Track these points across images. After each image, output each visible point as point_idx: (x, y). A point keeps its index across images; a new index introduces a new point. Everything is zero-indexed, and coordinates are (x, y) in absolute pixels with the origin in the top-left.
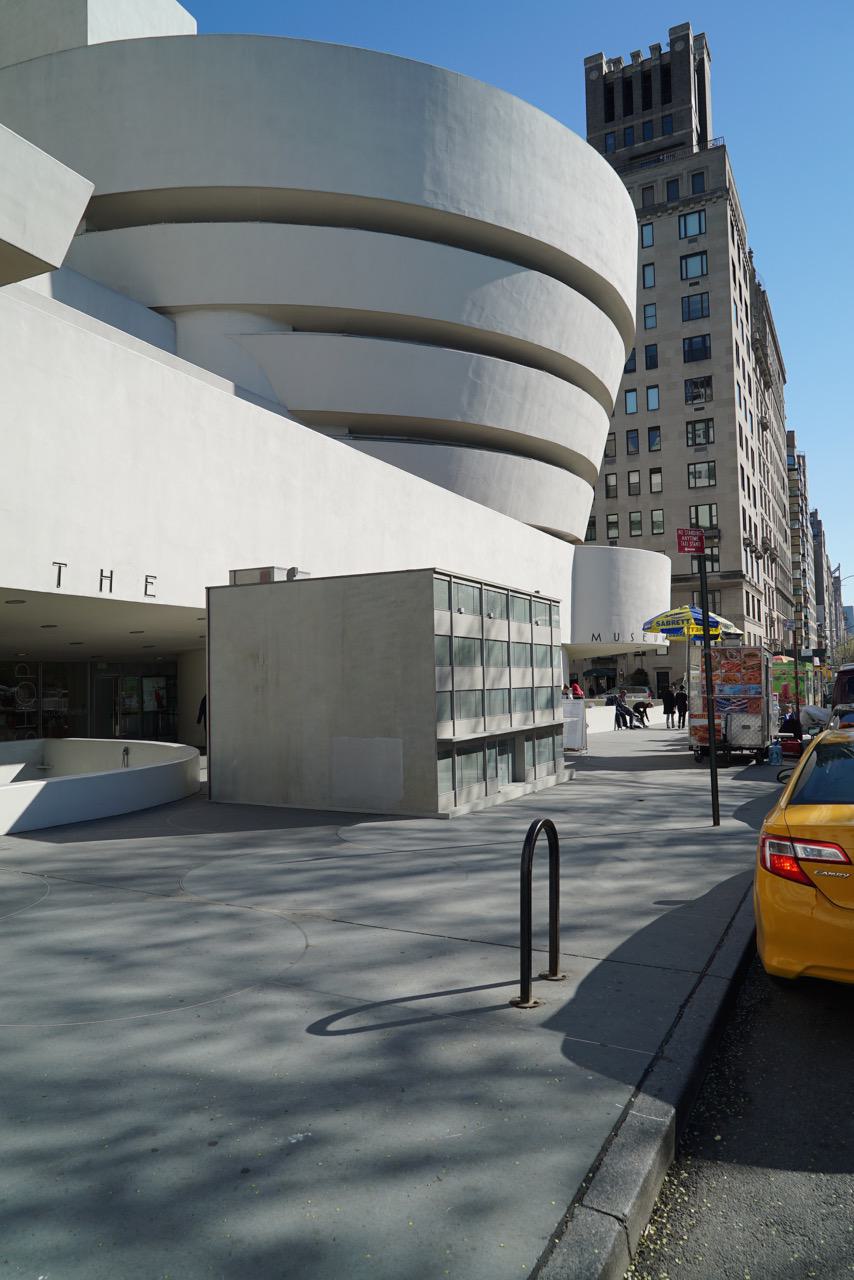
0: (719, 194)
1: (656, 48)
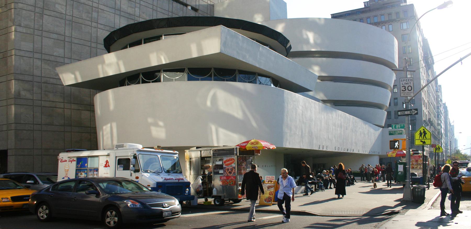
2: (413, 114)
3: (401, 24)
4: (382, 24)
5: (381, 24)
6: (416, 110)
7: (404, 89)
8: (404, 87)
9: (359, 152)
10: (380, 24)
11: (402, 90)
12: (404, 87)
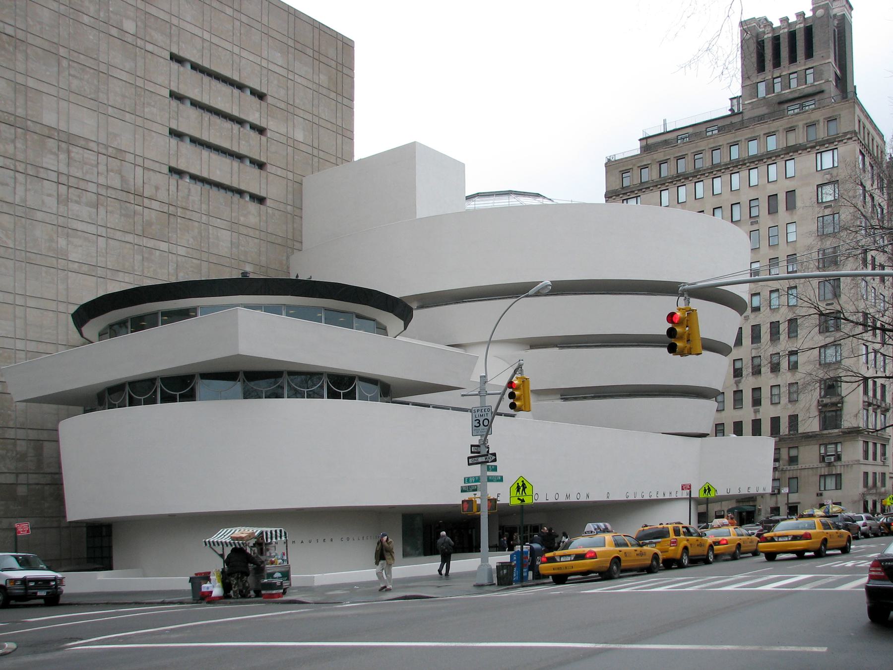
0: (849, 136)
1: (801, 15)
3: (819, 155)
4: (768, 158)
5: (765, 161)
7: (478, 425)
8: (478, 421)
10: (762, 160)
11: (475, 426)
12: (478, 421)
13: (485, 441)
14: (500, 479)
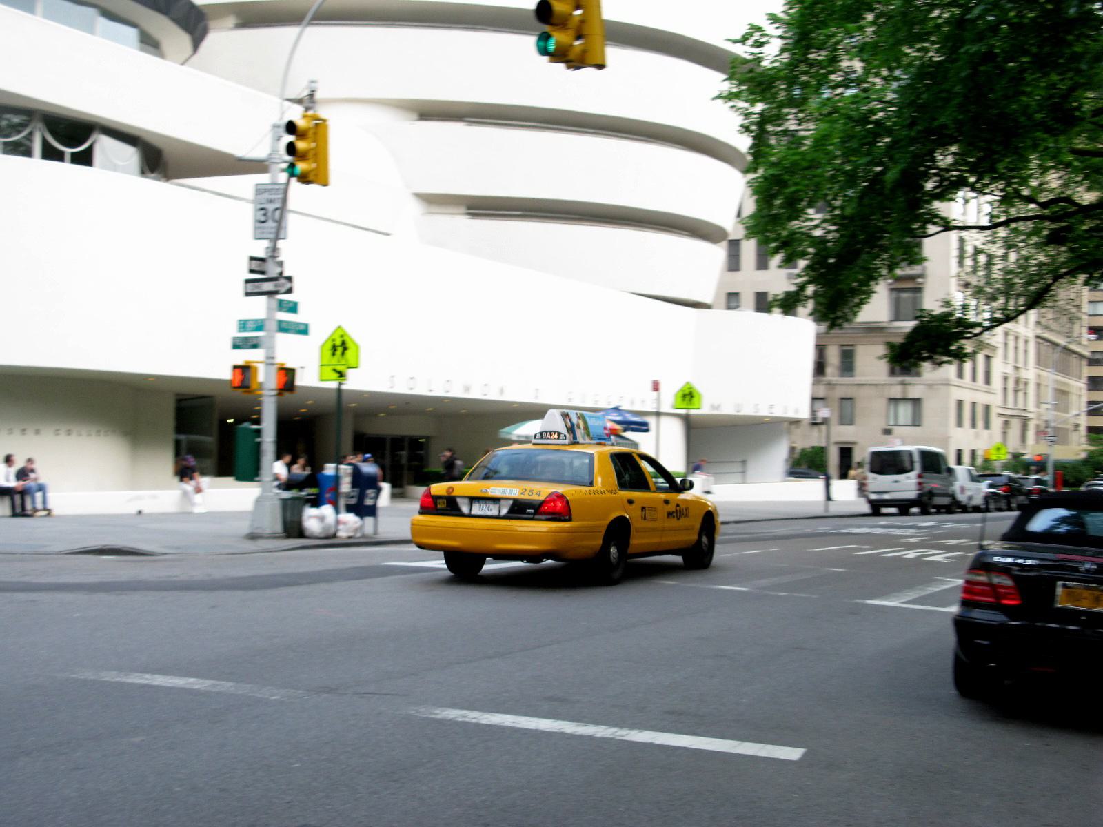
2: (283, 290)
6: (289, 279)
9: (536, 397)
13: (274, 250)
14: (303, 330)
